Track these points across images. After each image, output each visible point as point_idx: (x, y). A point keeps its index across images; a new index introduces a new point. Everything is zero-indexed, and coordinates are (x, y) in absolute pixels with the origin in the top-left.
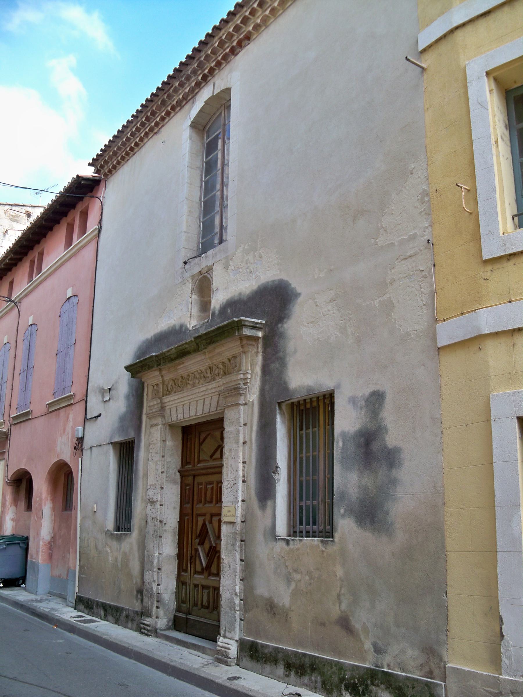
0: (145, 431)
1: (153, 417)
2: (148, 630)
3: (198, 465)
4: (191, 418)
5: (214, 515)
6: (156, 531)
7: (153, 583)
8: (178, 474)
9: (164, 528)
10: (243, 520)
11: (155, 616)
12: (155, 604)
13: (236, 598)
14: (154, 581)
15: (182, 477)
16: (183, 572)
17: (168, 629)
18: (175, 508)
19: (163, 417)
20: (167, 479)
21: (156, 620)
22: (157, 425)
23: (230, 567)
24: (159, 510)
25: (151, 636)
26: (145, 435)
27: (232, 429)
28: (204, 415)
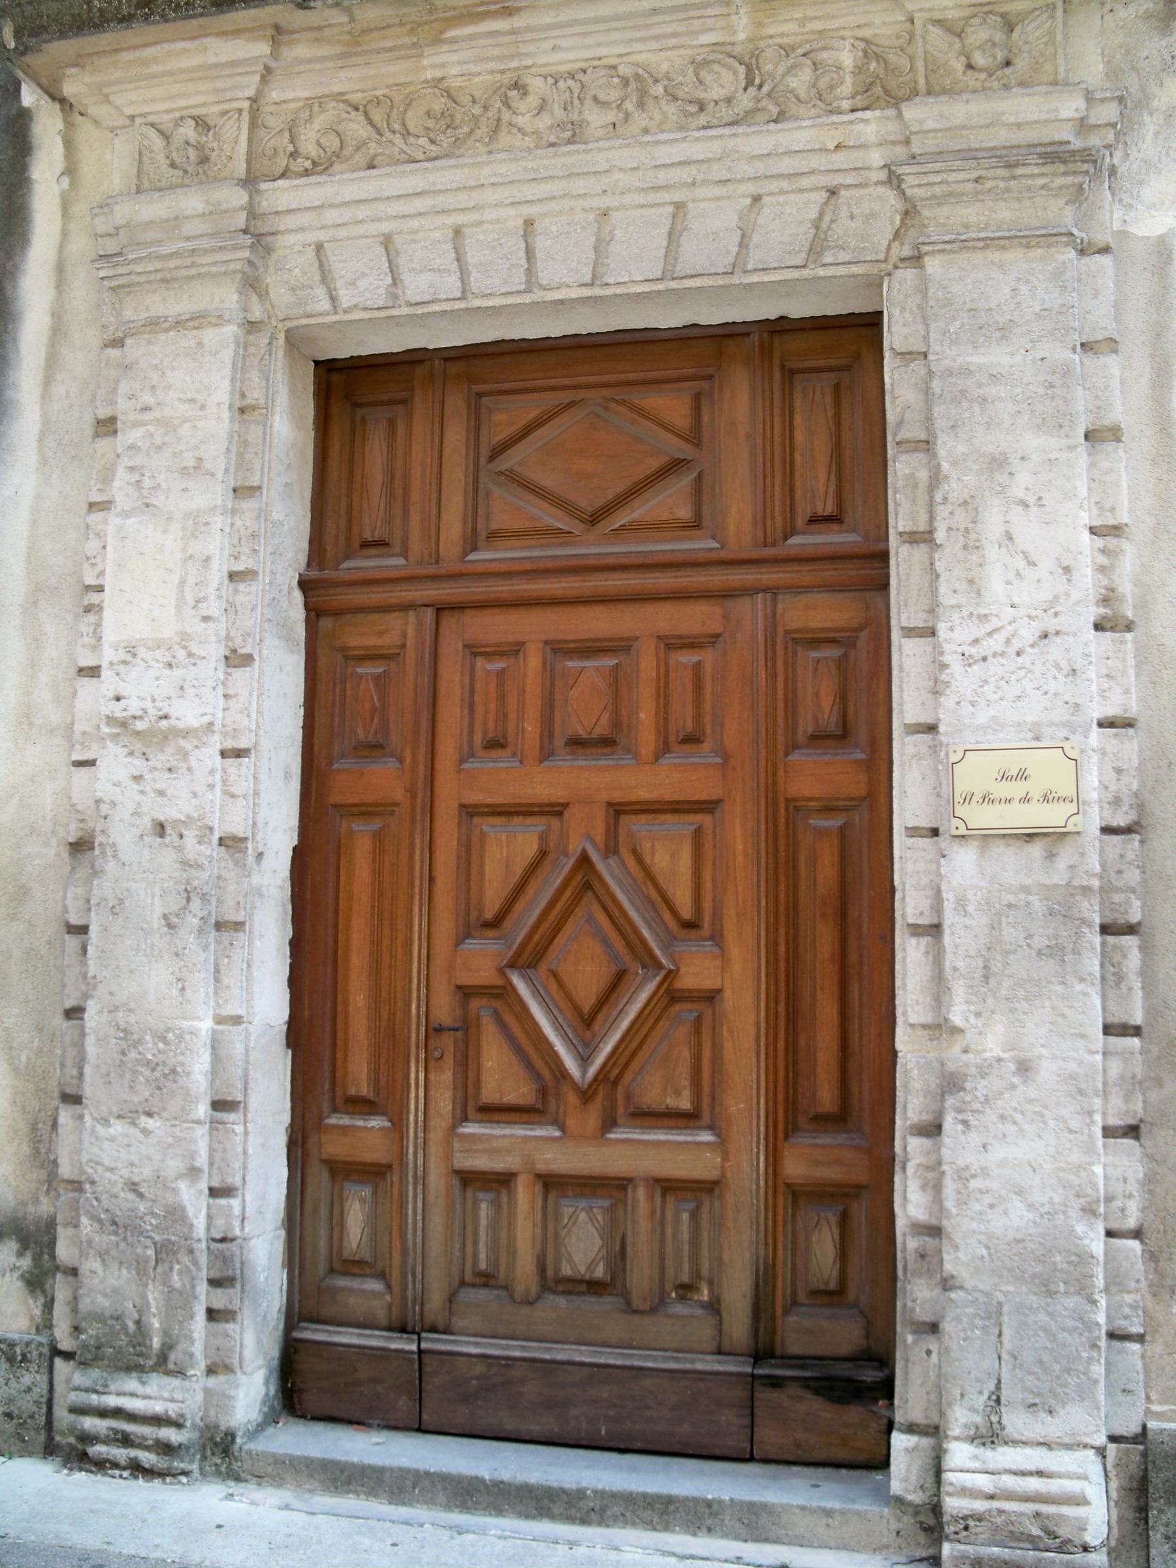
0: (52, 363)
1: (164, 280)
2: (166, 1449)
3: (471, 557)
4: (538, 296)
5: (626, 812)
6: (204, 897)
7: (182, 1185)
8: (298, 596)
9: (256, 880)
10: (1121, 821)
11: (203, 1365)
12: (203, 1298)
13: (1091, 1226)
14: (193, 1172)
15: (314, 613)
16: (335, 1110)
17: (270, 1419)
18: (287, 776)
19: (252, 284)
20: (269, 614)
21: (212, 1382)
22: (199, 320)
23: (1024, 1068)
24: (218, 776)
25: (185, 1473)
26: (48, 381)
27: (1006, 360)
28: (597, 291)
